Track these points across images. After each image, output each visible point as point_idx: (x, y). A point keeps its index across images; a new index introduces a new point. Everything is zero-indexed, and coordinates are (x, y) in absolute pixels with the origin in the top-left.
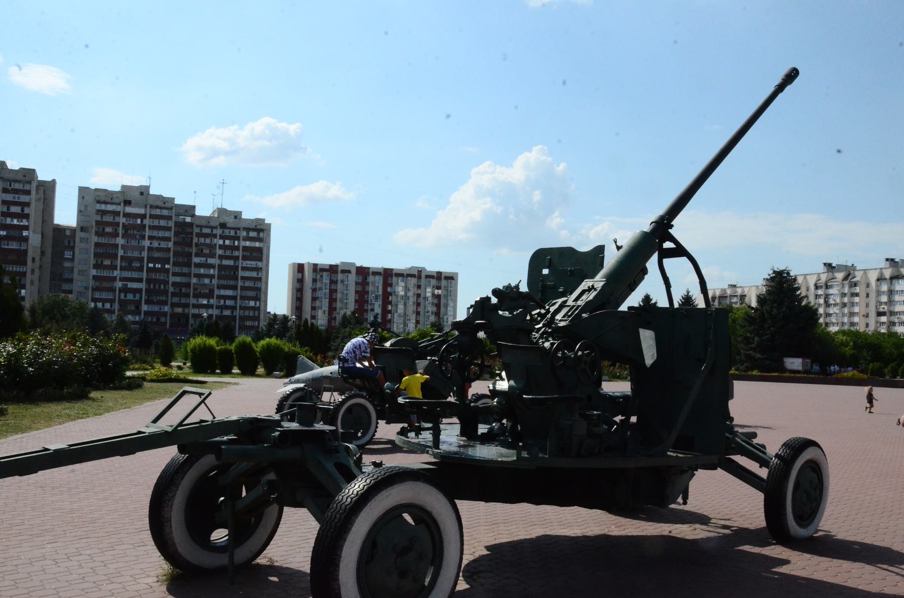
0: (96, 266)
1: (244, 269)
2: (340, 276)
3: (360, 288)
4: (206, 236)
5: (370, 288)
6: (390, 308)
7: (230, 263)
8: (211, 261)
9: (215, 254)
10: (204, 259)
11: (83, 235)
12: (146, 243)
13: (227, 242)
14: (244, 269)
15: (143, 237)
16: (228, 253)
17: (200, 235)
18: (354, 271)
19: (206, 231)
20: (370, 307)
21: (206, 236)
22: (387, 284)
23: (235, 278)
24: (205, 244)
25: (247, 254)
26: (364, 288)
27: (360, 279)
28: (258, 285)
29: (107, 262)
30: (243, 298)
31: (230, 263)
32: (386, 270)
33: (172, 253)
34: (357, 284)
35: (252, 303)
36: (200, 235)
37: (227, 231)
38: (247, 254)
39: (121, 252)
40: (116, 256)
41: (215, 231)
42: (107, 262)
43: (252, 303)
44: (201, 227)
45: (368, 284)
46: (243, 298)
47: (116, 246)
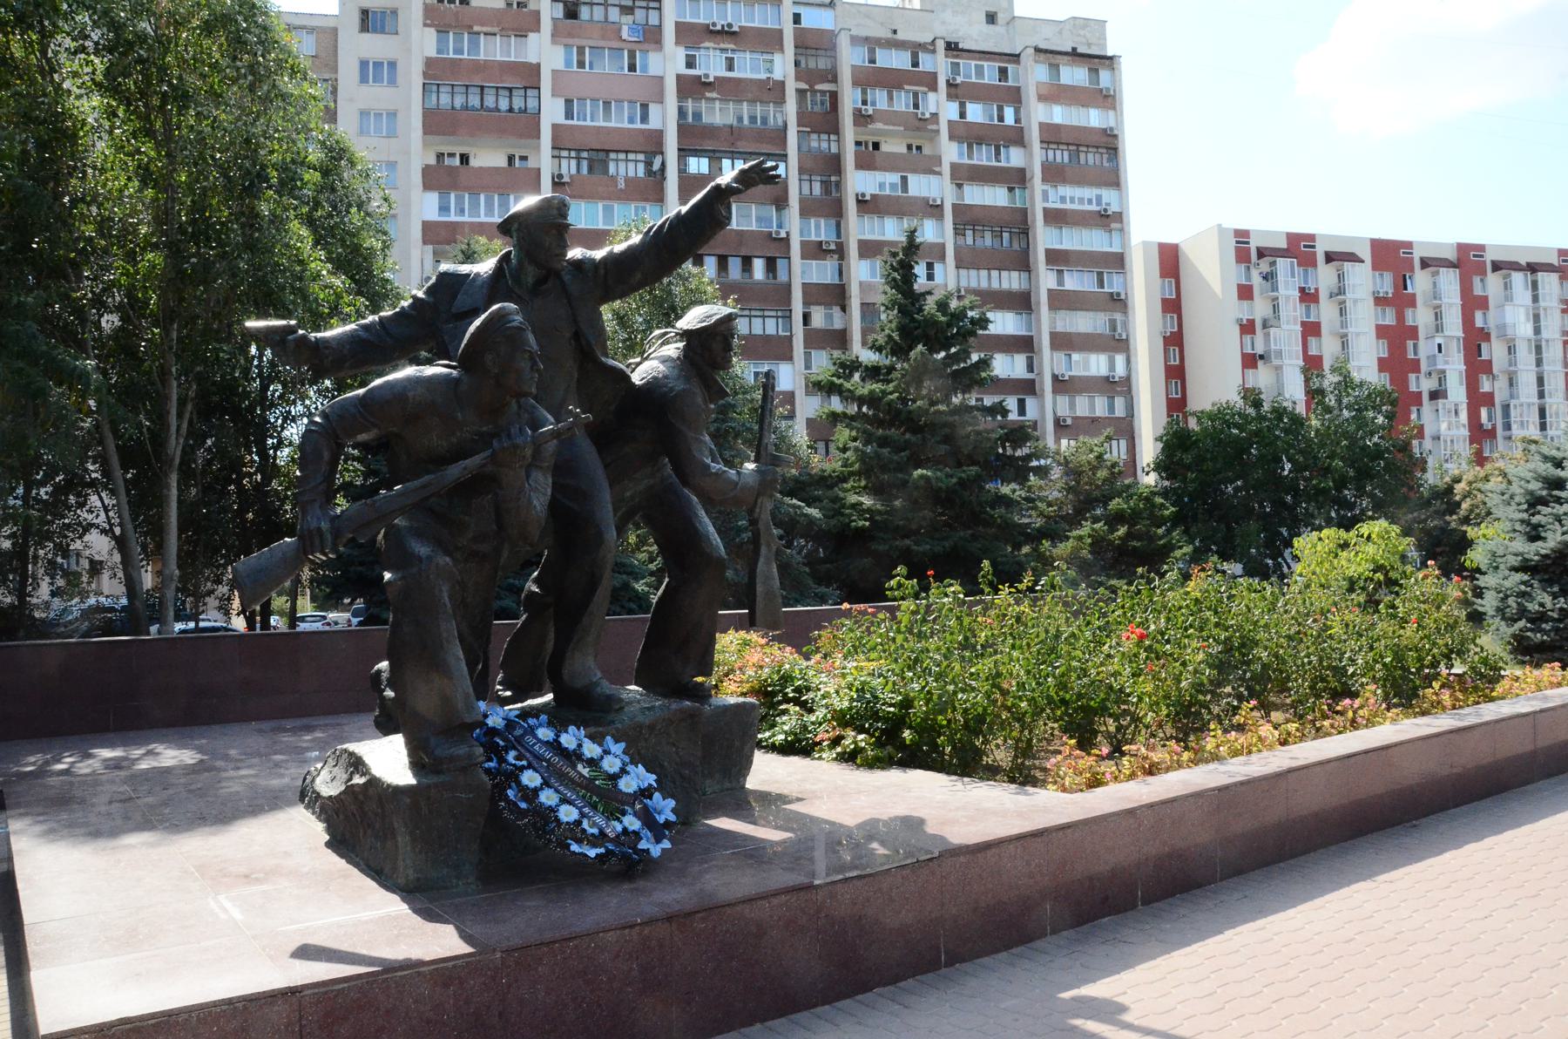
0: (435, 178)
1: (1056, 218)
2: (1324, 277)
3: (1389, 319)
4: (891, 81)
5: (1421, 317)
6: (1486, 386)
7: (994, 196)
8: (921, 186)
9: (938, 160)
10: (894, 178)
11: (375, 46)
12: (669, 62)
13: (976, 113)
14: (1056, 218)
15: (653, 36)
16: (983, 157)
17: (870, 78)
18: (1366, 254)
19: (899, 60)
20: (1427, 385)
21: (891, 81)
22: (1472, 303)
23: (1023, 262)
24: (890, 117)
25: (1061, 156)
26: (1400, 317)
27: (1387, 286)
28: (1114, 284)
29: (488, 157)
30: (1063, 342)
31: (994, 196)
32: (1463, 248)
33: (791, 106)
34: (1380, 301)
35: (1096, 365)
36: (870, 78)
37: (968, 67)
38: (1061, 156)
39: (552, 112)
40: (529, 124)
41: (926, 63)
42: (488, 157)
43: (1096, 365)
44: (872, 44)
45: (1411, 302)
46: (1063, 342)
47: (529, 75)
